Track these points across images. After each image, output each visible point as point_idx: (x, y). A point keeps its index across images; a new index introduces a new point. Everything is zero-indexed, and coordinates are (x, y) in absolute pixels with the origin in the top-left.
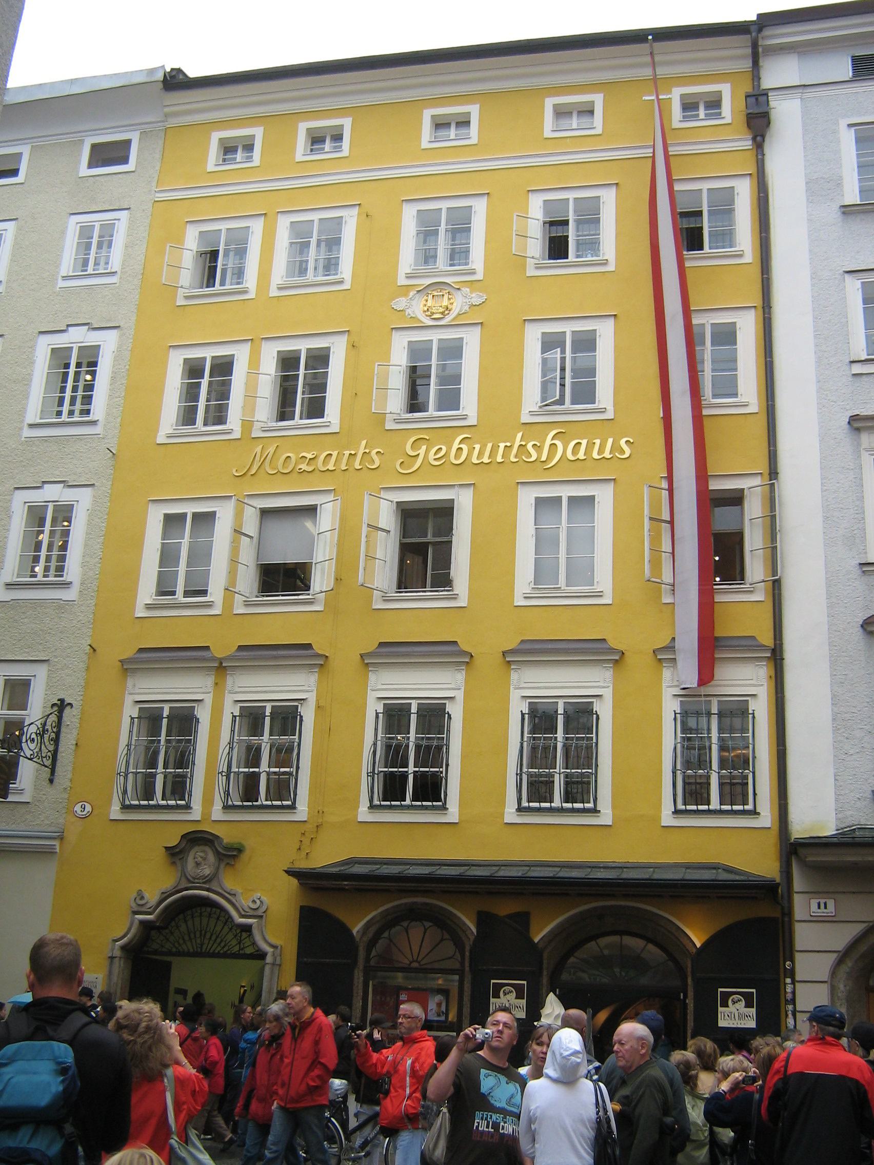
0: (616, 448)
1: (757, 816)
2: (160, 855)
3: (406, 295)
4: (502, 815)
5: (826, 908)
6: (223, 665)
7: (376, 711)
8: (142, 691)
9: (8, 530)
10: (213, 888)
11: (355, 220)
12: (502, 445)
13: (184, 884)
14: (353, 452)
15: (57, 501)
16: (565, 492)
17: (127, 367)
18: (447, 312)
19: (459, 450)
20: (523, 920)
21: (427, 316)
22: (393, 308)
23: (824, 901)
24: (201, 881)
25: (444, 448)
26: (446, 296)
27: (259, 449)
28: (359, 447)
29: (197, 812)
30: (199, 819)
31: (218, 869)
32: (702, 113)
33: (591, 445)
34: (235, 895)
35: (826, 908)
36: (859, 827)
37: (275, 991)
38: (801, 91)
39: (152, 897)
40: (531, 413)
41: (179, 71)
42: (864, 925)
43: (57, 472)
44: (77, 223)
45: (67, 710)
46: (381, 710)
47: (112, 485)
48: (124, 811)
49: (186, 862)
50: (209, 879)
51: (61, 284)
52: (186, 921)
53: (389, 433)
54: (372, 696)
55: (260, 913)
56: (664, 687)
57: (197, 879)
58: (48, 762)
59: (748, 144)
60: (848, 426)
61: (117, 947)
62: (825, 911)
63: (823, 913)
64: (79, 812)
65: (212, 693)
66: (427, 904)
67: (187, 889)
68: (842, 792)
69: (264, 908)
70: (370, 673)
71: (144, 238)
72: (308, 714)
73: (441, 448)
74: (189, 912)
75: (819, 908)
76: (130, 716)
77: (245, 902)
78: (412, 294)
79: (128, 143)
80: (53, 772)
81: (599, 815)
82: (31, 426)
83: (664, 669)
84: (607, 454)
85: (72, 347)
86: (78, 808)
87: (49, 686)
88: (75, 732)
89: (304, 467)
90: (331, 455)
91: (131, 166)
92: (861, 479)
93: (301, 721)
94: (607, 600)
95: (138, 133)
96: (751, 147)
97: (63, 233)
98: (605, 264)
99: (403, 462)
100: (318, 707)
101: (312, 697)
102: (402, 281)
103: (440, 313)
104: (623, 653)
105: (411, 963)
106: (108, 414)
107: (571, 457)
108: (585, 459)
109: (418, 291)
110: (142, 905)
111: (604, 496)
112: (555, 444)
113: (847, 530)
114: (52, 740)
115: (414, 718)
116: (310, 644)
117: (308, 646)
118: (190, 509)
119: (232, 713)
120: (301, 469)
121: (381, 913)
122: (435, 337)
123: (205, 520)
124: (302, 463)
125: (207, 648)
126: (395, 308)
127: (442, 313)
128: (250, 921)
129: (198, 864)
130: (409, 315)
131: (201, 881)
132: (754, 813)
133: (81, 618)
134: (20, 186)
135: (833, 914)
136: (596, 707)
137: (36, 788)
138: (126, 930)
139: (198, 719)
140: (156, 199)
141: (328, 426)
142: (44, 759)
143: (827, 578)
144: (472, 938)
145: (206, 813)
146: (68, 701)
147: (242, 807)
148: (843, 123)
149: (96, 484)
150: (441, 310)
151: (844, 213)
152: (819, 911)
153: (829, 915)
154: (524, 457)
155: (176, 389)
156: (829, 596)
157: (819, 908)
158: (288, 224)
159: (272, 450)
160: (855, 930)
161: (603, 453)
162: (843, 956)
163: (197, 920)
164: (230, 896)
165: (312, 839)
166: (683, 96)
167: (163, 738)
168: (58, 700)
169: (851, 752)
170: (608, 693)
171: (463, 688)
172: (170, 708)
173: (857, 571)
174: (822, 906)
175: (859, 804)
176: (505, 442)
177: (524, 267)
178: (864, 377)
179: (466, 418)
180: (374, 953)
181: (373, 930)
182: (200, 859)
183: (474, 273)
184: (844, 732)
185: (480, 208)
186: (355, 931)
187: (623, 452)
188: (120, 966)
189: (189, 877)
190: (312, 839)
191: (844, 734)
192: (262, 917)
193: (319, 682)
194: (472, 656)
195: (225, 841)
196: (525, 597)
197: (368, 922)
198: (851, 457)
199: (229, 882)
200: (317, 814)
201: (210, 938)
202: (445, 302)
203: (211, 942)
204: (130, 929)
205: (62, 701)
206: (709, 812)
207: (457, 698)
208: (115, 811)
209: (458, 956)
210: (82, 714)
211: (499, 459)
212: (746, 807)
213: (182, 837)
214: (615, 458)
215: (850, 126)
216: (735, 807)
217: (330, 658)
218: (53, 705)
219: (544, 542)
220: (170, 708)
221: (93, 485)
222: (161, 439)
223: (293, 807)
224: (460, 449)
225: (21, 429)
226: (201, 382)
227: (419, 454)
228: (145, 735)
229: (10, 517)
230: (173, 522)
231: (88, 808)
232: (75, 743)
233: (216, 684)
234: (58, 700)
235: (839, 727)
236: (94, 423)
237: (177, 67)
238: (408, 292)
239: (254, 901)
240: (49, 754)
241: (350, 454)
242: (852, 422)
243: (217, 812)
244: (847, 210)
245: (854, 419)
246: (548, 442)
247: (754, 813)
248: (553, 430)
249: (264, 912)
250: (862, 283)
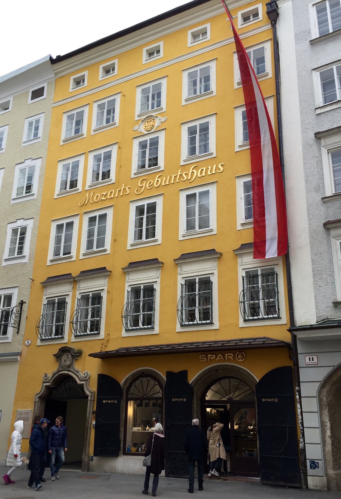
0: (217, 168)
1: (280, 319)
2: (53, 358)
3: (138, 124)
4: (175, 329)
5: (313, 360)
6: (75, 280)
7: (127, 290)
8: (49, 294)
9: (6, 239)
10: (70, 370)
11: (120, 98)
12: (173, 176)
13: (61, 369)
14: (120, 189)
15: (21, 226)
16: (197, 191)
17: (44, 172)
18: (153, 127)
20: (184, 374)
21: (145, 130)
23: (312, 357)
24: (66, 367)
25: (152, 182)
26: (152, 121)
27: (87, 195)
28: (122, 187)
29: (66, 340)
30: (67, 342)
31: (73, 361)
32: (251, 19)
33: (207, 169)
34: (78, 372)
35: (313, 360)
36: (327, 320)
37: (92, 412)
39: (50, 375)
40: (184, 161)
41: (59, 56)
42: (332, 368)
43: (22, 215)
44: (28, 121)
45: (24, 304)
46: (129, 289)
47: (40, 217)
48: (42, 342)
49: (61, 360)
50: (69, 366)
51: (23, 145)
52: (65, 386)
53: (133, 179)
54: (127, 285)
55: (87, 378)
56: (238, 266)
57: (65, 367)
58: (16, 326)
59: (269, 26)
60: (315, 138)
61: (37, 397)
62: (313, 362)
63: (312, 363)
64: (27, 344)
65: (72, 292)
66: (148, 370)
67: (61, 371)
68: (319, 305)
69: (88, 377)
70: (126, 276)
71: (49, 122)
72: (104, 295)
73: (151, 182)
74: (66, 381)
75: (310, 360)
76: (43, 304)
77: (82, 375)
78: (140, 123)
79: (43, 88)
80: (19, 329)
81: (213, 325)
82: (14, 199)
83: (238, 258)
84: (214, 172)
85: (26, 168)
86: (26, 342)
87: (18, 296)
88: (26, 313)
89: (103, 198)
90: (112, 192)
91: (45, 96)
92: (322, 160)
93: (102, 298)
94: (214, 233)
95: (47, 83)
96: (271, 27)
97: (23, 126)
98: (212, 93)
99: (137, 190)
100: (108, 292)
101: (106, 288)
102: (137, 118)
103: (150, 128)
104: (222, 254)
105: (144, 396)
106: (38, 191)
107: (199, 176)
108: (205, 176)
109: (142, 121)
110: (46, 379)
111: (213, 189)
112: (193, 172)
113: (316, 185)
114: (17, 317)
115: (142, 291)
116: (105, 267)
117: (105, 268)
118: (64, 222)
119: (77, 298)
120: (102, 199)
121: (131, 375)
122: (148, 138)
123: (70, 225)
125: (70, 274)
127: (151, 128)
128: (83, 382)
129: (65, 361)
131: (66, 367)
132: (279, 318)
133: (29, 269)
134: (10, 112)
135: (317, 363)
136: (212, 279)
137: (13, 336)
138: (41, 390)
139: (67, 302)
140: (53, 107)
141: (111, 181)
142: (12, 325)
143: (307, 208)
144: (165, 383)
145: (69, 339)
146: (24, 301)
147: (81, 336)
148: (310, 5)
149: (34, 218)
150: (150, 127)
151: (311, 44)
152: (310, 362)
153: (315, 363)
156: (309, 214)
157: (310, 360)
158: (97, 106)
159: (92, 194)
160: (327, 371)
161: (212, 171)
162: (324, 385)
163: (68, 383)
164: (76, 373)
165: (105, 346)
166: (242, 14)
167: (56, 311)
168: (21, 301)
169: (322, 285)
170: (216, 272)
171: (160, 277)
172: (58, 299)
173: (321, 202)
174: (311, 359)
175: (327, 309)
178: (322, 115)
179: (160, 168)
180: (130, 393)
181: (128, 382)
182: (65, 358)
183: (162, 109)
184: (318, 277)
185: (164, 82)
186: (121, 384)
187: (220, 169)
188: (38, 405)
189: (62, 366)
190: (105, 346)
191: (318, 277)
192: (87, 380)
193: (109, 281)
194: (163, 264)
195: (75, 350)
196: (183, 237)
197: (126, 379)
198: (317, 151)
199: (77, 366)
200: (107, 336)
201: (72, 391)
202: (152, 123)
203: (73, 392)
204: (42, 389)
205: (22, 301)
206: (259, 319)
207: (158, 281)
208: (39, 343)
209: (161, 392)
210: (29, 305)
211: (172, 182)
212: (275, 316)
213: (59, 350)
214: (217, 173)
215: (313, 5)
216: (270, 316)
217: (112, 272)
218: (19, 303)
219: (190, 213)
220: (58, 299)
221: (33, 218)
222: (55, 197)
223: (99, 334)
224: (158, 180)
225: (10, 201)
228: (52, 310)
229: (6, 235)
230: (60, 227)
231: (30, 342)
232: (26, 317)
233: (73, 287)
234: (21, 301)
235: (316, 274)
236: (33, 195)
237: (58, 55)
238: (139, 122)
239: (85, 374)
240: (15, 322)
241: (119, 190)
242: (316, 136)
243: (73, 339)
244: (313, 42)
245: (316, 134)
247: (279, 318)
249: (89, 378)
250: (320, 73)
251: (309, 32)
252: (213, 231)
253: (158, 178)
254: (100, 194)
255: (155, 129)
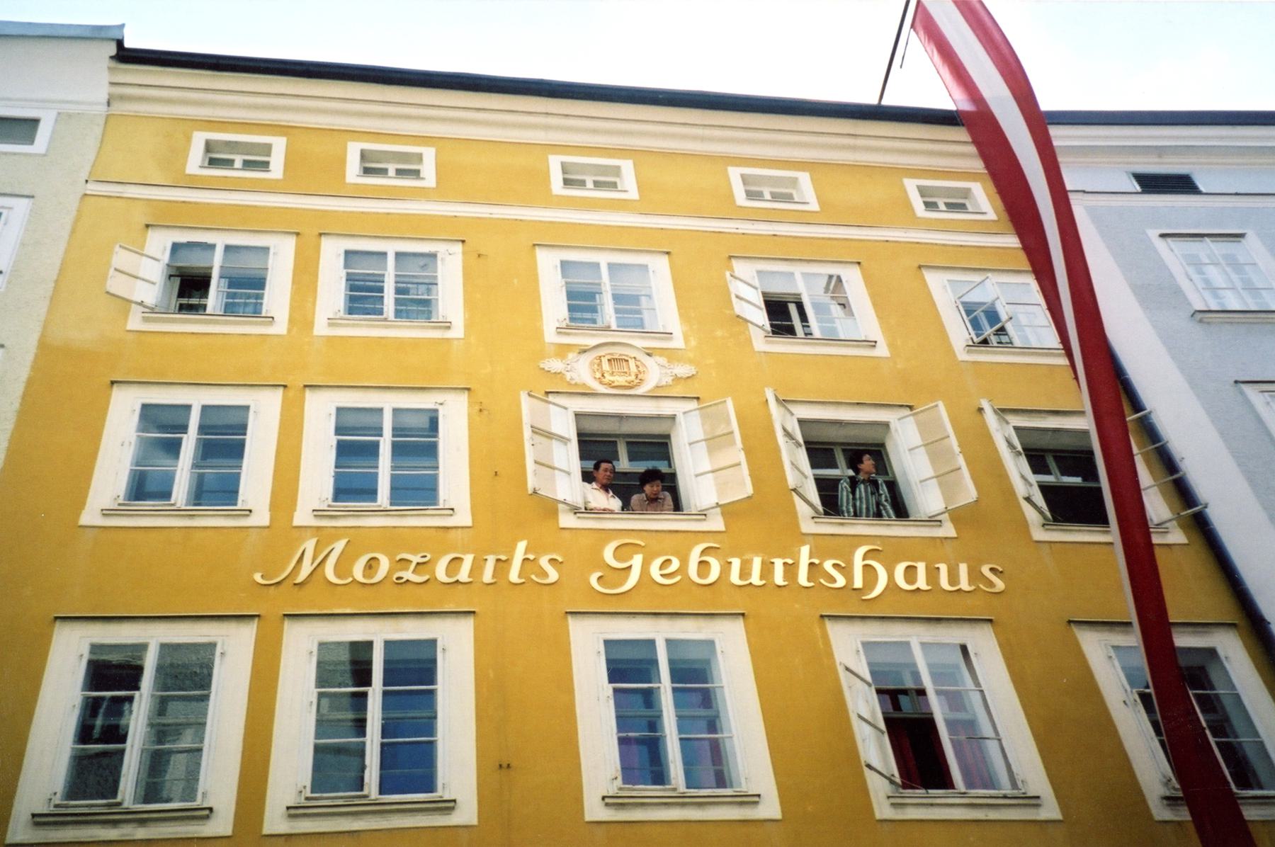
12: (779, 564)
14: (503, 558)
19: (703, 566)
22: (543, 369)
25: (675, 564)
27: (310, 545)
38: (1080, 197)
73: (669, 561)
89: (408, 575)
99: (600, 578)
120: (401, 578)
124: (401, 570)
126: (546, 369)
130: (572, 379)
140: (88, 192)
141: (451, 515)
148: (1153, 234)
150: (629, 378)
154: (822, 581)
155: (126, 444)
176: (783, 559)
177: (749, 341)
224: (703, 564)
226: (181, 439)
227: (630, 567)
241: (498, 560)
244: (1202, 316)
246: (858, 562)
248: (864, 545)
251: (1178, 291)
252: (1038, 806)
253: (704, 552)
254: (390, 556)
255: (649, 391)
